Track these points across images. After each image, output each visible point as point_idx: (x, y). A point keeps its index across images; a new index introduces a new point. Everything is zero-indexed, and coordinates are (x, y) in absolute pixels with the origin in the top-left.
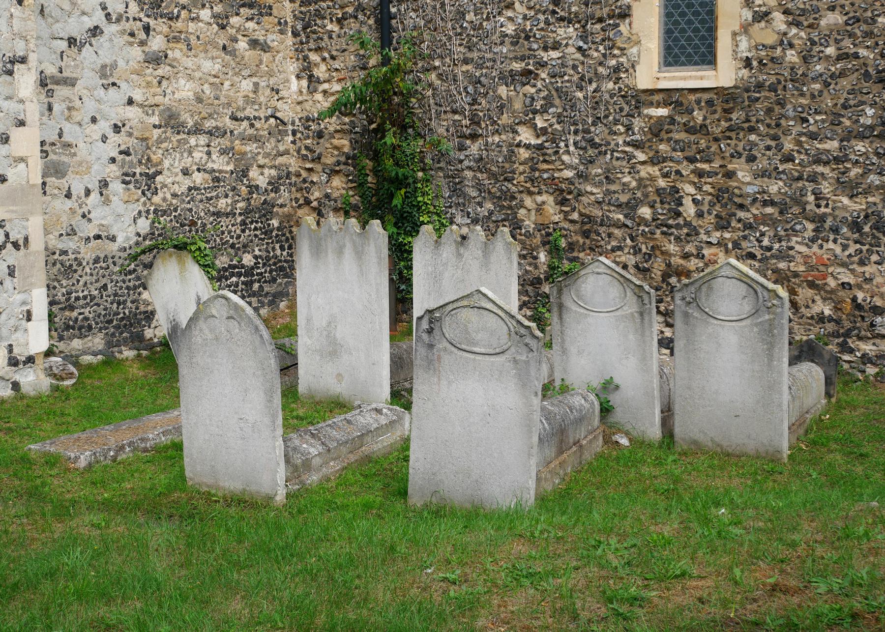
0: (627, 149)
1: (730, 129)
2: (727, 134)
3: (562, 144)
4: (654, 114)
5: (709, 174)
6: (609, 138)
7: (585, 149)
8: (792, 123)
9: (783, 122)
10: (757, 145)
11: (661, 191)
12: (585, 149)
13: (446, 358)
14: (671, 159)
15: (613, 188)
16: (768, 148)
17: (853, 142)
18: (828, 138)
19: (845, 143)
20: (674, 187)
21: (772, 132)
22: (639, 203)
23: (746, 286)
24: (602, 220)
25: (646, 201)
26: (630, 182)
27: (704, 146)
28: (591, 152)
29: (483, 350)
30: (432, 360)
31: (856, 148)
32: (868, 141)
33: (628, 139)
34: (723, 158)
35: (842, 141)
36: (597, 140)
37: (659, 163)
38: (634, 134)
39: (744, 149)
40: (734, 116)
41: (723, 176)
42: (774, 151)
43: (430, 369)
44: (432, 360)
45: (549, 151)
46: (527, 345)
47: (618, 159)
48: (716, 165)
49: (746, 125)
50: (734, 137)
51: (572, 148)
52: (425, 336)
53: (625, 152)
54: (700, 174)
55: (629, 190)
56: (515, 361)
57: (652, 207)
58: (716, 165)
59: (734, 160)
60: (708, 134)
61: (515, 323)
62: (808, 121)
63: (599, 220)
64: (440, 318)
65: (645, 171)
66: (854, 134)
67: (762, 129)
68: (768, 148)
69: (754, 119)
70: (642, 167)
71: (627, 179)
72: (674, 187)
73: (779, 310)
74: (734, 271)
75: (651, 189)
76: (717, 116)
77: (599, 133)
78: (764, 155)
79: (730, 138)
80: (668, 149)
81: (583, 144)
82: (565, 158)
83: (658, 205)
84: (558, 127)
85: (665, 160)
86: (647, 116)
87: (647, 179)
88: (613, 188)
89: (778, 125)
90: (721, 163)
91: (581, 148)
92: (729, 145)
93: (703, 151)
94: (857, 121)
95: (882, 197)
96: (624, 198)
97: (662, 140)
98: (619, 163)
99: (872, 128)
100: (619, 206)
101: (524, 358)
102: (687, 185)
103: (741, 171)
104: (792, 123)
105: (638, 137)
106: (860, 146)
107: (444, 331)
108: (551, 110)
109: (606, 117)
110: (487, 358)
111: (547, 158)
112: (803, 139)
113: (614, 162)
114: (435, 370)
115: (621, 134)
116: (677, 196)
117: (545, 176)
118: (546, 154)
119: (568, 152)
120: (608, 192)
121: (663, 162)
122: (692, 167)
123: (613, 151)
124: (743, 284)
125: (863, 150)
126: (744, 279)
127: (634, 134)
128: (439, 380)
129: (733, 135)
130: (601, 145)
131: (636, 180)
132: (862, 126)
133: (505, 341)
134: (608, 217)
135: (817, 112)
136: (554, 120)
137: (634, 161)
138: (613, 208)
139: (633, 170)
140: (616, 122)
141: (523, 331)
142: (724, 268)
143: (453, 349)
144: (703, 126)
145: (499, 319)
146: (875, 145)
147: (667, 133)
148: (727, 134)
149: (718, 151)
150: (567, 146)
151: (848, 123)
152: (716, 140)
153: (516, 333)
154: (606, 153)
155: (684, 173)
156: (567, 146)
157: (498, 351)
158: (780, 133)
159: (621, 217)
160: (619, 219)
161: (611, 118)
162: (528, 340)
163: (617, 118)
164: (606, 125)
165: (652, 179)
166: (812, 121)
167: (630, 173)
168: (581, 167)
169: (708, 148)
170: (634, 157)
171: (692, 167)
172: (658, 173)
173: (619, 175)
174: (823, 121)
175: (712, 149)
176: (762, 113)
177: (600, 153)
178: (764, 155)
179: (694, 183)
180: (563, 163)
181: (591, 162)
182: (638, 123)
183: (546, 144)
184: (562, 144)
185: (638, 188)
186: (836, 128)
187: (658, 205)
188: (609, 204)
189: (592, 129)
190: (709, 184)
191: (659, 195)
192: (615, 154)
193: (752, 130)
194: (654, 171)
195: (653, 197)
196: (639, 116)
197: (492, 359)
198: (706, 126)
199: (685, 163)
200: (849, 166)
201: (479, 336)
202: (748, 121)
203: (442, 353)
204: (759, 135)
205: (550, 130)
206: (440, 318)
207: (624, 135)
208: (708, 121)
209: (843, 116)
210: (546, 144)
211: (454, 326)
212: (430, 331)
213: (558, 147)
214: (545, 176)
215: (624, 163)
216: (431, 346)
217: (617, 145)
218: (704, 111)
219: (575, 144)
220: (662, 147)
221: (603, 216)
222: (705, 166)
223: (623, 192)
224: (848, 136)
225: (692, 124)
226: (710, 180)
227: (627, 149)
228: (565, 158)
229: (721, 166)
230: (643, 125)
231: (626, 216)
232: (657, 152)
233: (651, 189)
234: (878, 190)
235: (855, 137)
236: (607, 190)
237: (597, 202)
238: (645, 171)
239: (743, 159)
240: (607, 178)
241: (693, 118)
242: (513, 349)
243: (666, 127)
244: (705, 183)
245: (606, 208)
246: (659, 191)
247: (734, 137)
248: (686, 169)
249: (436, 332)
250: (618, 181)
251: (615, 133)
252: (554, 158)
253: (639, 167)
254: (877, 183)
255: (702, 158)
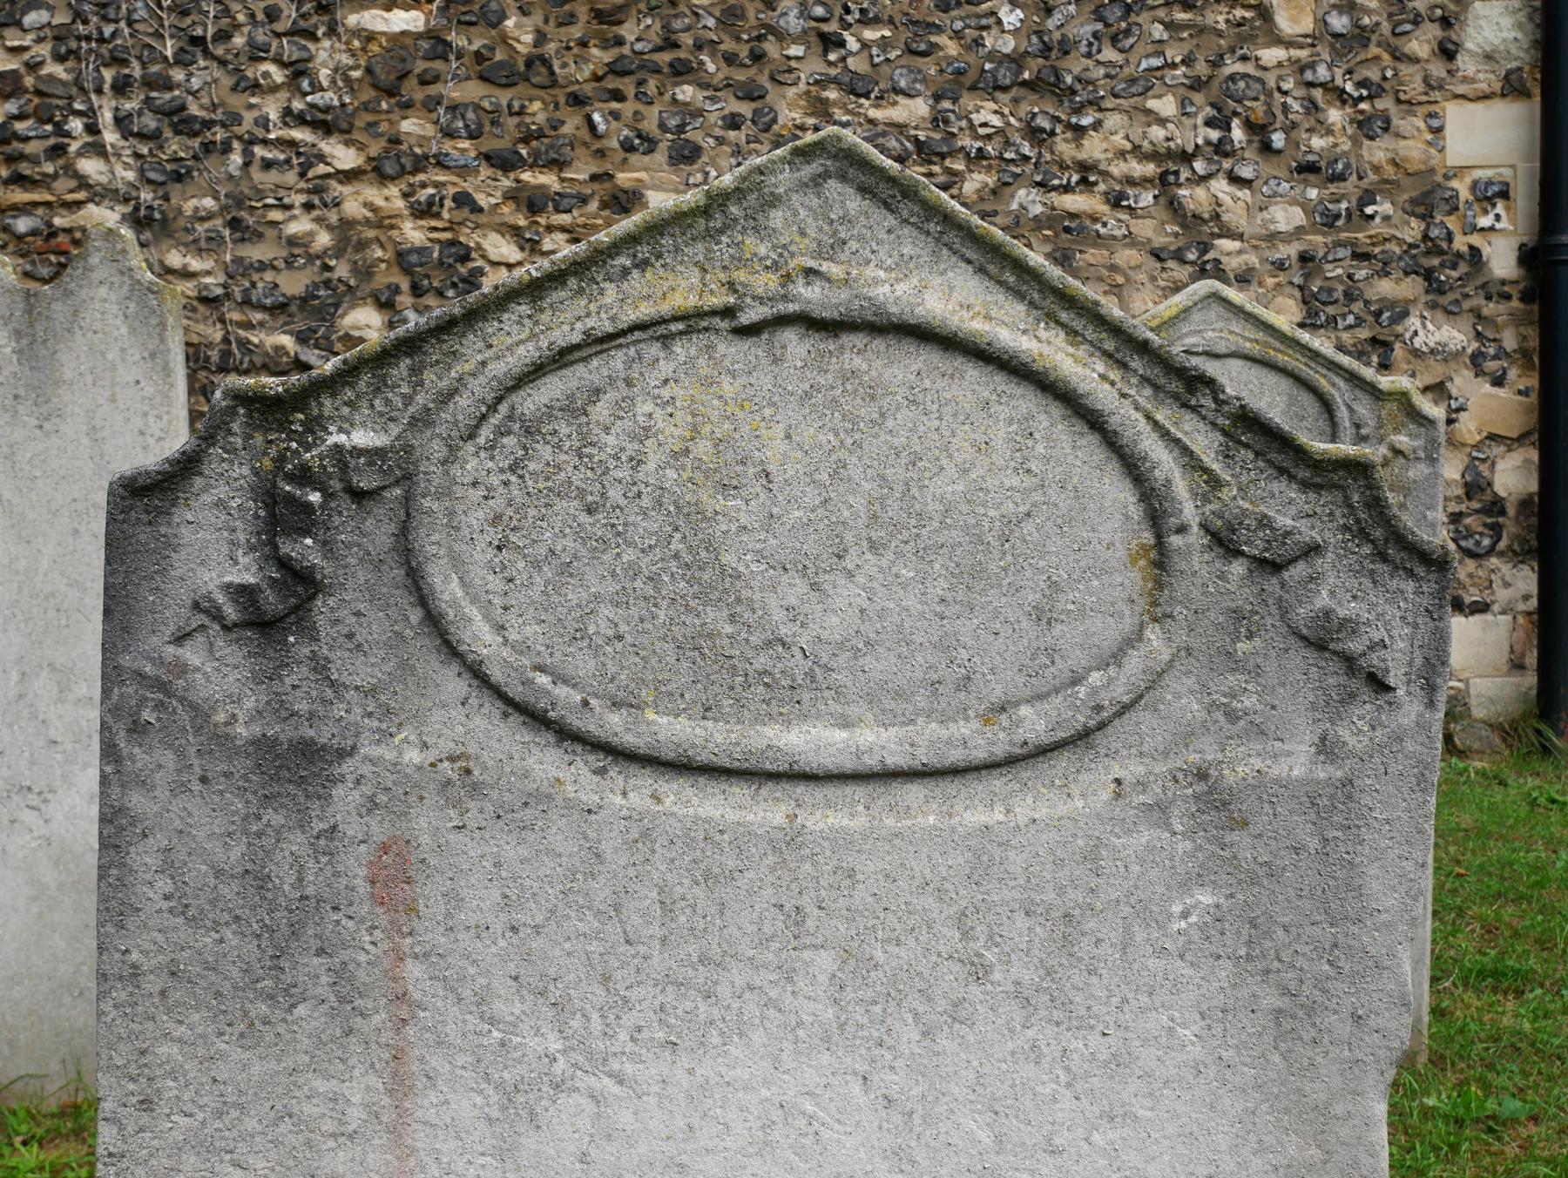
0: (298, 134)
1: (615, 69)
2: (612, 83)
3: (76, 125)
4: (380, 26)
5: (559, 203)
6: (236, 102)
7: (153, 137)
8: (796, 50)
9: (771, 47)
10: (700, 113)
11: (414, 258)
12: (153, 137)
13: (472, 870)
14: (441, 163)
15: (255, 253)
16: (733, 122)
17: (968, 101)
18: (897, 91)
19: (946, 104)
20: (453, 243)
21: (740, 76)
22: (345, 295)
23: (1284, 384)
24: (225, 354)
25: (366, 288)
26: (311, 234)
27: (541, 118)
28: (175, 145)
29: (878, 742)
30: (307, 906)
31: (977, 118)
32: (1004, 97)
33: (298, 105)
34: (601, 154)
35: (937, 98)
36: (194, 109)
37: (403, 172)
38: (317, 87)
39: (663, 126)
40: (628, 31)
41: (604, 205)
42: (747, 129)
43: (289, 996)
44: (307, 906)
45: (33, 148)
46: (1321, 640)
47: (268, 165)
48: (580, 171)
49: (665, 58)
50: (630, 90)
51: (110, 137)
52: (219, 673)
53: (292, 143)
54: (533, 202)
55: (311, 258)
56: (1216, 802)
57: (386, 304)
58: (580, 171)
59: (635, 159)
60: (554, 84)
61: (1205, 443)
62: (842, 44)
63: (214, 355)
64: (399, 467)
65: (355, 202)
66: (968, 80)
67: (711, 67)
68: (733, 122)
69: (687, 39)
70: (346, 190)
71: (299, 226)
72: (453, 243)
73: (1418, 471)
74: (1236, 326)
75: (379, 253)
76: (576, 32)
77: (200, 84)
78: (721, 141)
79: (618, 96)
80: (430, 130)
81: (150, 122)
82: (90, 167)
83: (405, 300)
84: (58, 70)
85: (420, 163)
86: (357, 32)
87: (367, 222)
88: (255, 253)
89: (758, 57)
90: (594, 169)
91: (142, 136)
92: (616, 115)
93: (540, 135)
94: (978, 42)
95: (1048, 248)
96: (293, 284)
97: (408, 105)
98: (273, 177)
99: (1016, 60)
100: (280, 309)
101: (1296, 761)
102: (494, 237)
103: (657, 188)
104: (796, 50)
105: (329, 97)
106: (987, 114)
107: (447, 589)
108: (31, 19)
109: (223, 36)
110: (921, 807)
111: (25, 168)
112: (832, 94)
113: (257, 175)
114: (346, 993)
115: (275, 88)
116: (463, 270)
117: (22, 225)
118: (22, 157)
119: (98, 149)
120: (240, 269)
121: (417, 170)
122: (506, 183)
123: (252, 141)
124: (1272, 379)
125: (996, 121)
126: (1281, 359)
127: (317, 87)
128: (400, 1087)
129: (627, 86)
130: (208, 124)
131: (330, 228)
132: (991, 56)
133: (1107, 631)
134: (244, 344)
135: (866, 20)
136: (44, 50)
137: (322, 169)
138: (258, 316)
139: (318, 199)
140: (256, 53)
141: (1286, 508)
142: (1196, 316)
143: (547, 763)
144: (537, 60)
145: (1049, 420)
146: (1024, 109)
147: (424, 82)
148: (612, 83)
149: (584, 134)
150: (92, 129)
151: (952, 48)
152: (577, 100)
153: (1223, 542)
154: (226, 149)
155: (482, 200)
156: (92, 129)
157: (1034, 724)
158: (764, 80)
159: (286, 341)
160: (280, 349)
161: (239, 41)
162: (1337, 588)
163: (260, 37)
164: (223, 63)
165: (382, 221)
166: (853, 44)
167: (308, 207)
168: (146, 195)
169: (555, 125)
170: (322, 158)
171: (506, 183)
172: (400, 204)
173: (276, 215)
174: (884, 44)
175: (567, 129)
176: (711, 22)
177: (208, 148)
178: (721, 141)
179: (515, 232)
180: (83, 182)
181: (178, 178)
182: (326, 56)
183: (20, 126)
184: (76, 125)
185: (339, 252)
186: (920, 62)
187: (405, 300)
188: (246, 303)
189: (178, 75)
190: (563, 229)
191: (407, 270)
192: (259, 151)
193: (681, 71)
194: (390, 198)
195: (386, 276)
196: (332, 31)
197: (977, 810)
198: (545, 62)
199: (485, 171)
200: (959, 166)
201: (837, 614)
202: (671, 44)
203: (427, 823)
204: (703, 86)
205: (29, 81)
206: (399, 467)
207: (283, 95)
208: (551, 48)
209: (939, 29)
210: (20, 126)
211: (561, 526)
212: (275, 615)
213: (60, 131)
214: (22, 225)
215: (291, 177)
216: (296, 766)
217: (264, 122)
218: (537, 18)
219: (121, 121)
220: (410, 126)
221: (226, 340)
222: (548, 179)
223: (289, 264)
224: (957, 84)
225: (499, 56)
226: (564, 219)
227: (298, 134)
228: (90, 167)
229: (594, 178)
230: (346, 59)
231: (302, 339)
232: (395, 141)
233: (379, 253)
234: (1039, 228)
235: (973, 88)
236: (238, 261)
237: (205, 300)
238: (355, 202)
239: (660, 156)
240: (235, 224)
241: (504, 39)
242: (1183, 700)
243: (420, 66)
244: (550, 229)
245: (236, 316)
246: (402, 258)
247: (630, 90)
248: (488, 190)
249: (357, 616)
250: (270, 233)
251: (255, 87)
252: (49, 168)
253: (337, 189)
254: (1037, 209)
255: (536, 154)
